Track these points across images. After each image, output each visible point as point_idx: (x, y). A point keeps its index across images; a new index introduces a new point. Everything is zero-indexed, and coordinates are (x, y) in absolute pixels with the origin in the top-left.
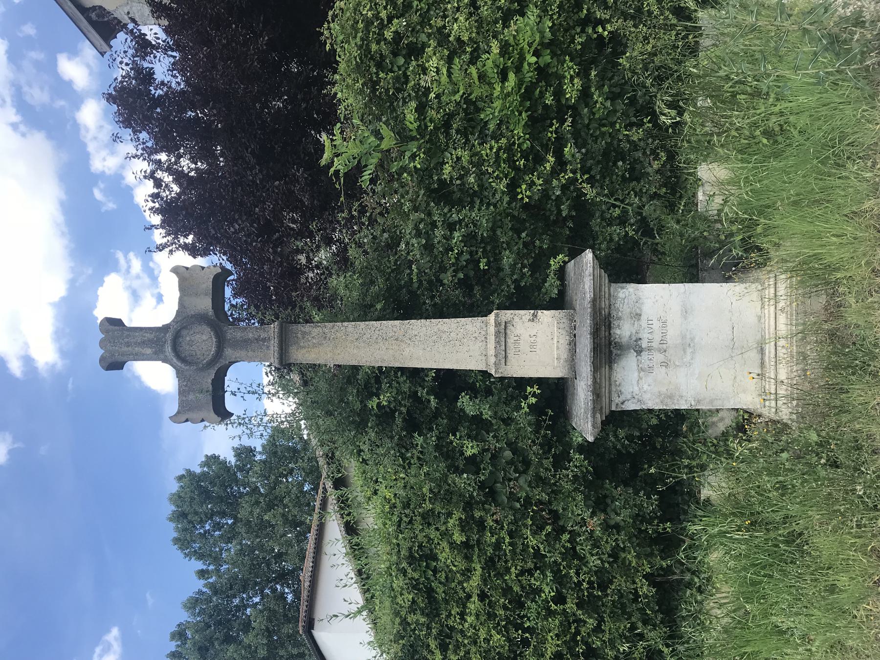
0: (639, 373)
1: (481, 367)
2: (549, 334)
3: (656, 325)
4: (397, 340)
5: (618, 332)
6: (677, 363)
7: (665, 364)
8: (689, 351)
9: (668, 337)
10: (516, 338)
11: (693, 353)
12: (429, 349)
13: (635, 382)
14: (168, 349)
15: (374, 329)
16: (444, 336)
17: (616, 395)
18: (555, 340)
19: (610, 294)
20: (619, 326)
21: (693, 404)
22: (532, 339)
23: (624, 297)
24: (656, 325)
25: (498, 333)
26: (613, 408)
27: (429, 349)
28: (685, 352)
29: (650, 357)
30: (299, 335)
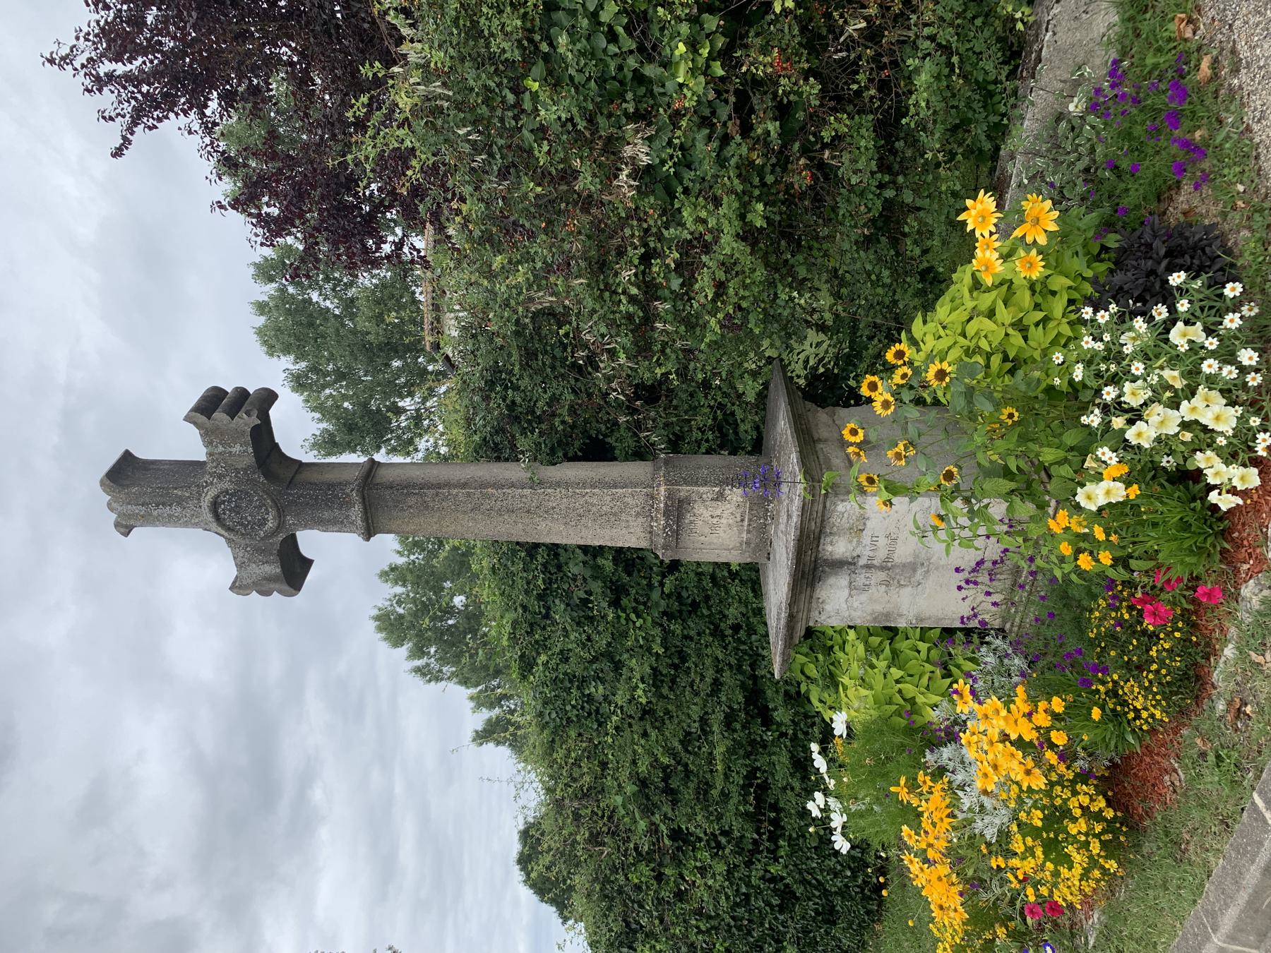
0: (851, 589)
1: (643, 544)
2: (738, 516)
3: (882, 542)
4: (528, 511)
5: (829, 548)
6: (902, 583)
7: (887, 584)
8: (920, 572)
9: (896, 555)
10: (692, 519)
11: (928, 571)
12: (573, 523)
13: (842, 600)
14: (209, 517)
15: (494, 499)
16: (594, 509)
17: (817, 613)
18: (746, 523)
19: (825, 507)
20: (831, 542)
21: (914, 622)
22: (715, 520)
23: (843, 510)
24: (882, 542)
25: (667, 514)
26: (811, 624)
27: (573, 523)
28: (914, 570)
29: (867, 575)
30: (390, 504)
